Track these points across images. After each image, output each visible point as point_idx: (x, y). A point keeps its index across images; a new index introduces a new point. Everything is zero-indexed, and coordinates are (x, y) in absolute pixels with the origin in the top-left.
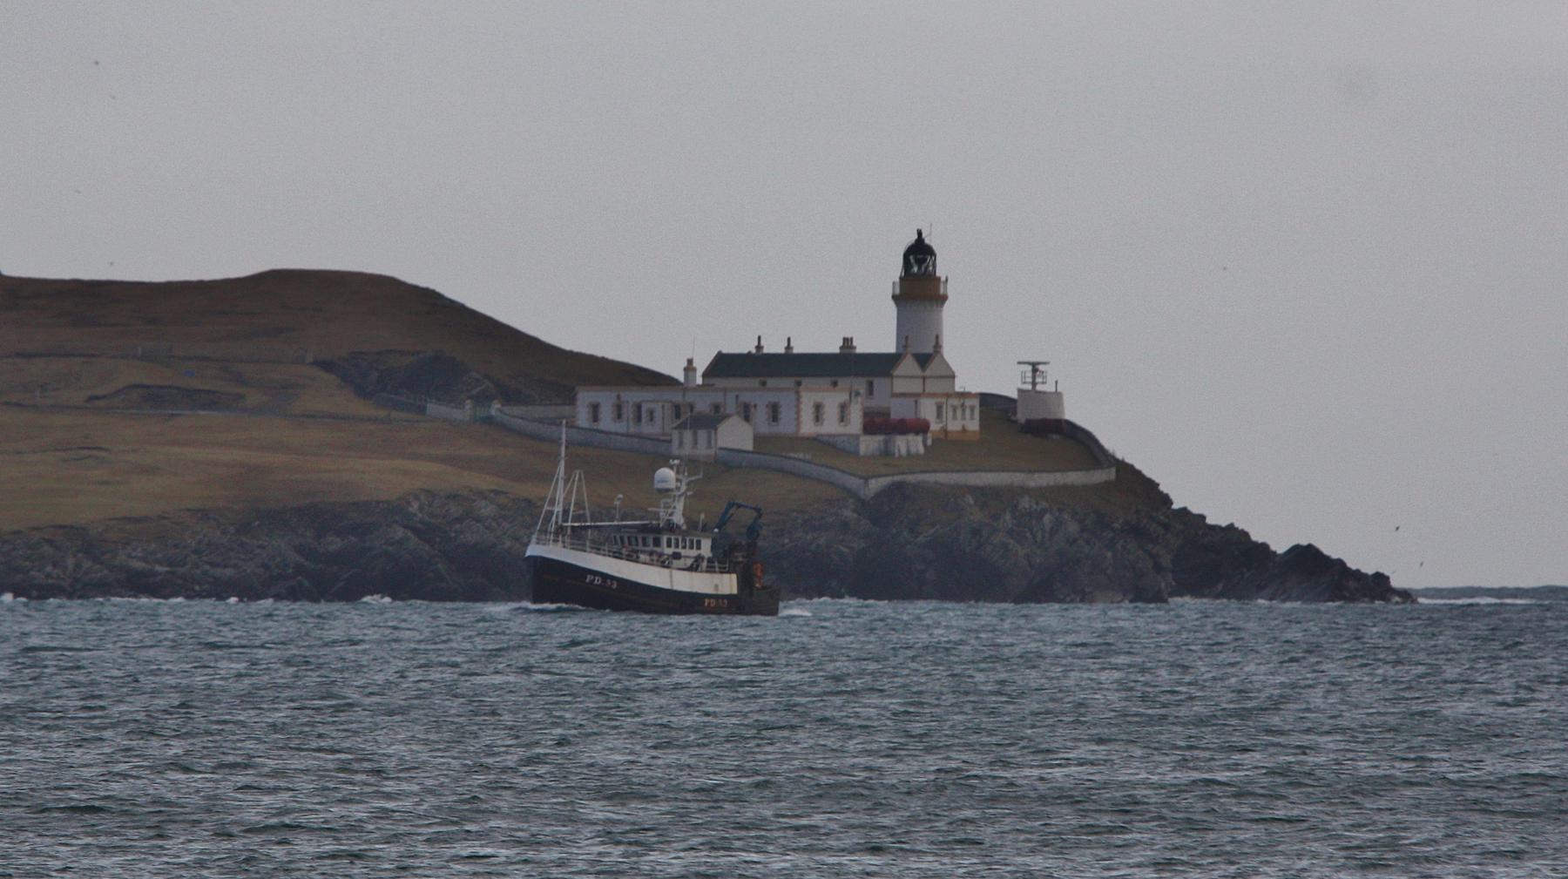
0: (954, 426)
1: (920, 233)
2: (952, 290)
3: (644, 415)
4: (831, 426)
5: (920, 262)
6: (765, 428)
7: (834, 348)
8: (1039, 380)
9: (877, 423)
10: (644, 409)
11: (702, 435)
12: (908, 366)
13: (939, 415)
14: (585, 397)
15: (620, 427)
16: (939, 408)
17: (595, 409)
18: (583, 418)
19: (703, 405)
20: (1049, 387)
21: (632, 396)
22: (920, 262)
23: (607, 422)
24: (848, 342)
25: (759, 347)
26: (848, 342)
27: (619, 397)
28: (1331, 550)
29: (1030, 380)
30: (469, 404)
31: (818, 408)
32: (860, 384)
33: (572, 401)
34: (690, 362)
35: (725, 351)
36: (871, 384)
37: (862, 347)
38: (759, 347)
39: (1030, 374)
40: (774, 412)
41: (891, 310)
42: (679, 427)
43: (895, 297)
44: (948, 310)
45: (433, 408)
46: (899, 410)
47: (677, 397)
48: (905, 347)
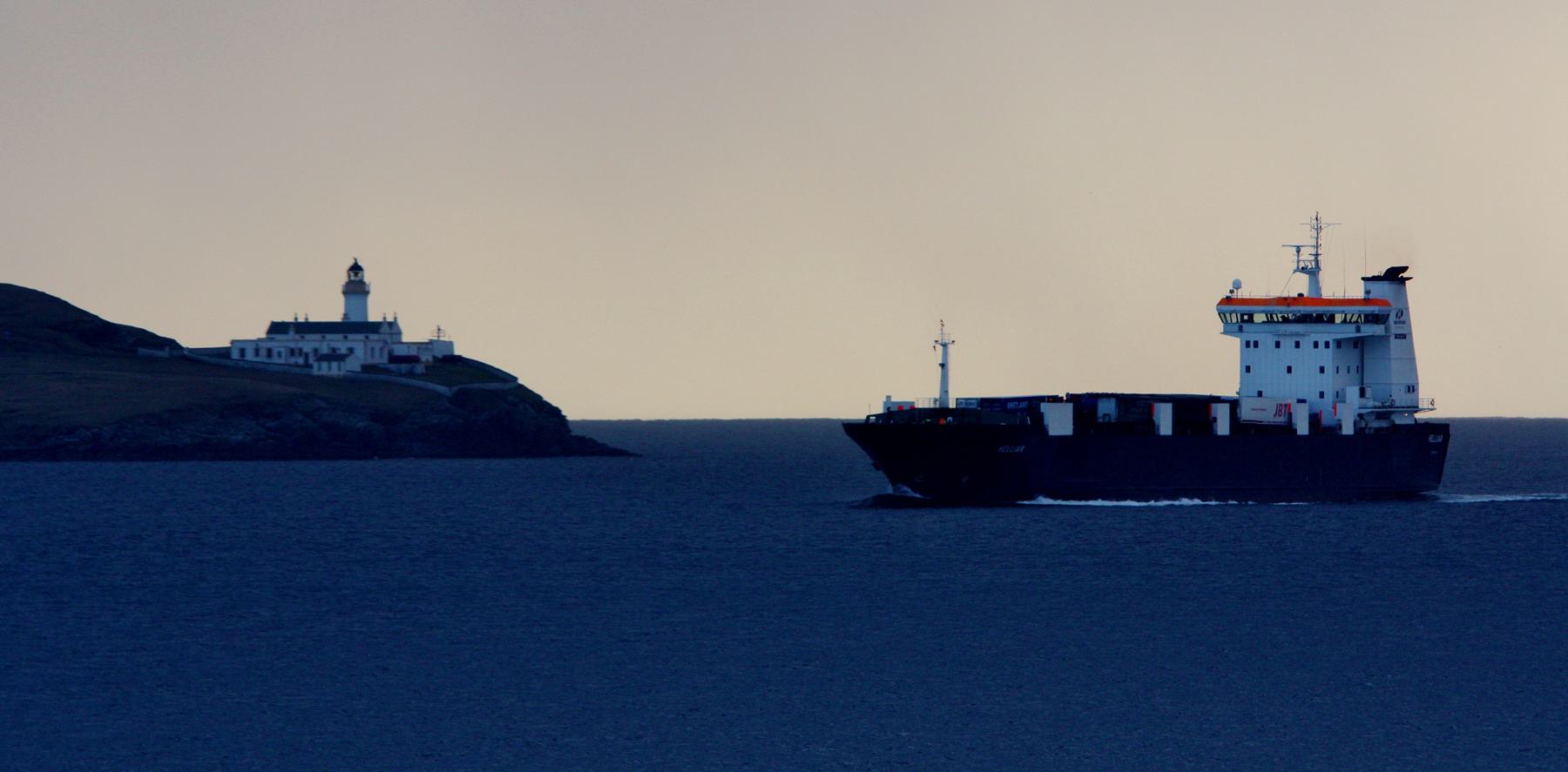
1: (356, 260)
2: (373, 289)
5: (356, 275)
20: (446, 339)
22: (356, 275)
29: (436, 335)
42: (316, 360)
43: (345, 293)
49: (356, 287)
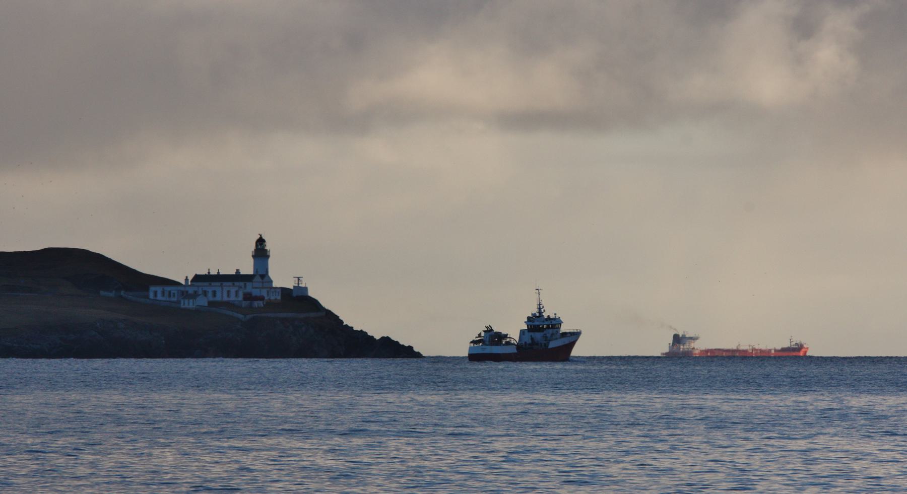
0: (273, 298)
1: (261, 236)
2: (271, 254)
3: (172, 294)
4: (233, 298)
5: (261, 245)
6: (211, 298)
7: (233, 272)
8: (300, 283)
9: (248, 297)
10: (172, 292)
11: (191, 301)
12: (258, 279)
13: (268, 295)
14: (153, 289)
15: (163, 299)
16: (268, 292)
17: (156, 293)
18: (151, 296)
19: (191, 291)
20: (302, 285)
21: (168, 289)
22: (261, 245)
23: (159, 297)
24: (238, 271)
25: (209, 273)
26: (238, 271)
27: (163, 289)
28: (394, 338)
29: (297, 283)
30: (114, 292)
31: (229, 292)
32: (242, 284)
33: (147, 290)
34: (187, 277)
35: (198, 273)
36: (245, 284)
37: (242, 273)
38: (209, 273)
39: (297, 281)
40: (214, 293)
41: (252, 261)
42: (183, 299)
43: (253, 256)
44: (270, 260)
45: (102, 293)
46: (256, 292)
47: (182, 289)
48: (257, 272)
49: (261, 252)
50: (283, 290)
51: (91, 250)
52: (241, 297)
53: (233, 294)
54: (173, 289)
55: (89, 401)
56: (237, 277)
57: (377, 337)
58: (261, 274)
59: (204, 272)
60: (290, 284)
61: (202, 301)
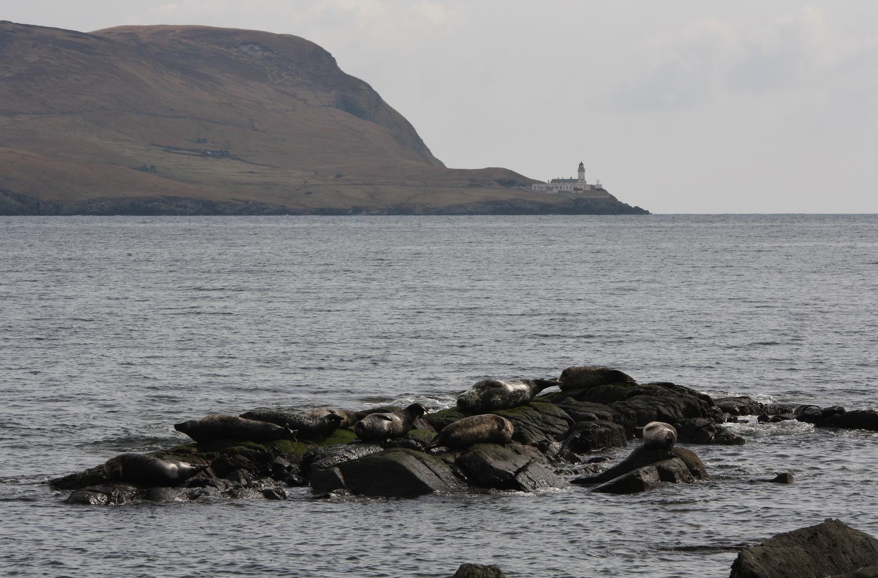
6: (559, 189)
7: (569, 178)
9: (576, 189)
12: (580, 181)
14: (534, 185)
17: (535, 187)
19: (550, 186)
20: (600, 184)
21: (540, 185)
23: (537, 189)
28: (640, 207)
31: (567, 187)
37: (573, 178)
40: (561, 187)
44: (586, 173)
46: (579, 187)
49: (581, 168)
50: (591, 185)
51: (345, 72)
52: (572, 189)
53: (568, 188)
54: (542, 185)
55: (474, 325)
56: (571, 181)
57: (633, 207)
58: (582, 180)
59: (556, 178)
60: (594, 184)
61: (555, 191)
